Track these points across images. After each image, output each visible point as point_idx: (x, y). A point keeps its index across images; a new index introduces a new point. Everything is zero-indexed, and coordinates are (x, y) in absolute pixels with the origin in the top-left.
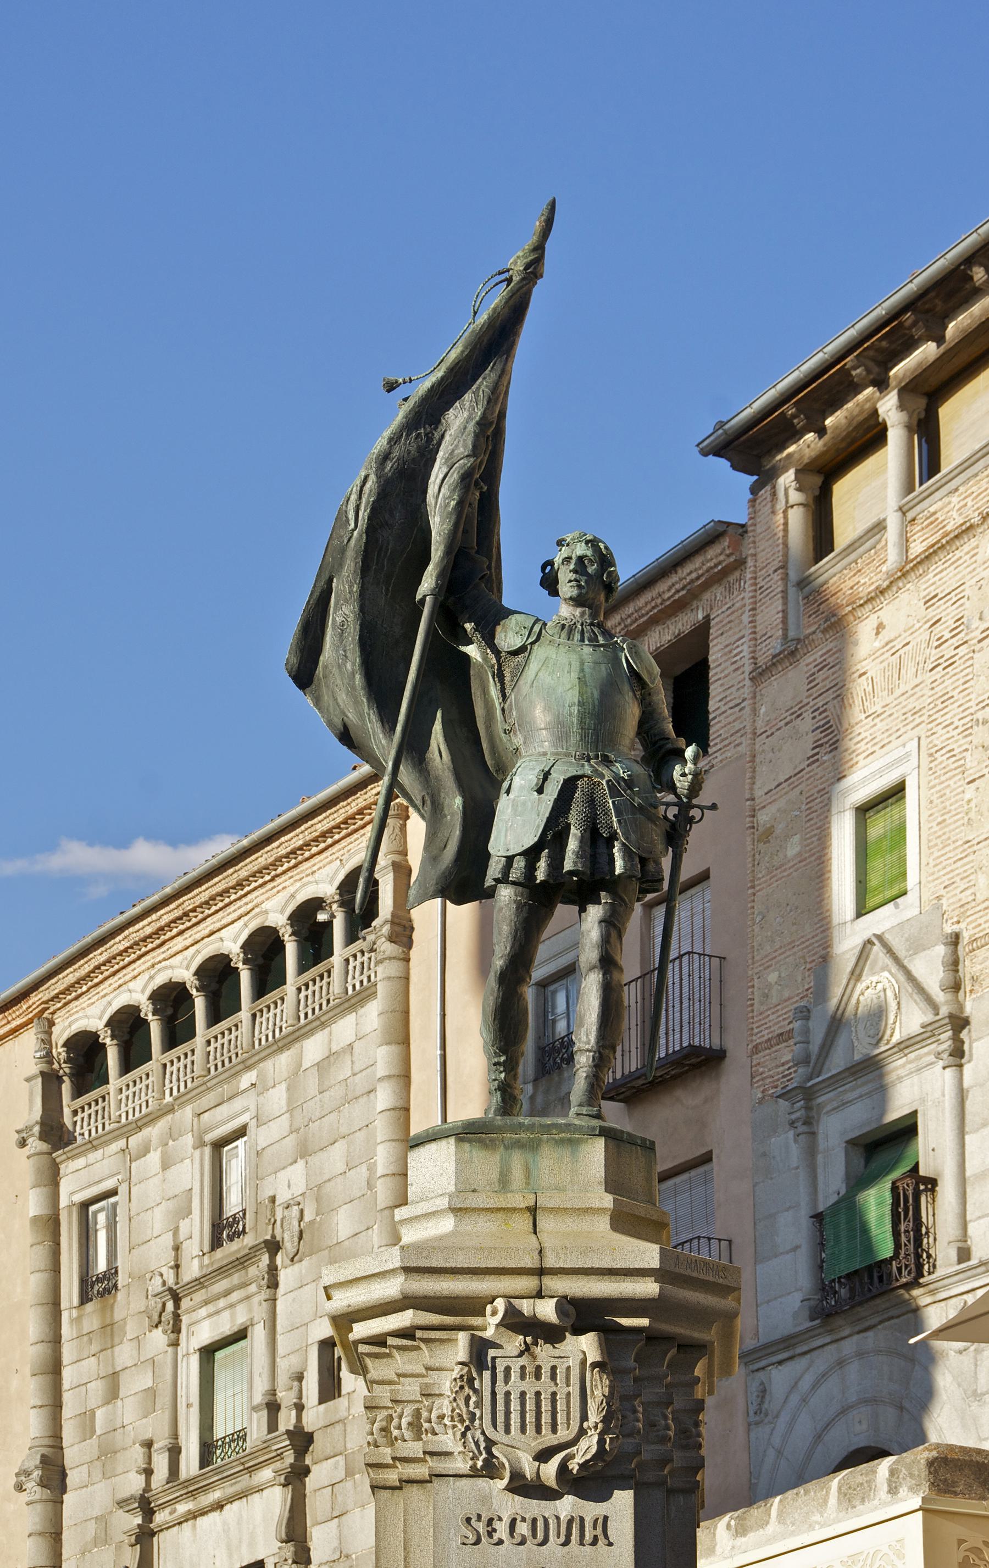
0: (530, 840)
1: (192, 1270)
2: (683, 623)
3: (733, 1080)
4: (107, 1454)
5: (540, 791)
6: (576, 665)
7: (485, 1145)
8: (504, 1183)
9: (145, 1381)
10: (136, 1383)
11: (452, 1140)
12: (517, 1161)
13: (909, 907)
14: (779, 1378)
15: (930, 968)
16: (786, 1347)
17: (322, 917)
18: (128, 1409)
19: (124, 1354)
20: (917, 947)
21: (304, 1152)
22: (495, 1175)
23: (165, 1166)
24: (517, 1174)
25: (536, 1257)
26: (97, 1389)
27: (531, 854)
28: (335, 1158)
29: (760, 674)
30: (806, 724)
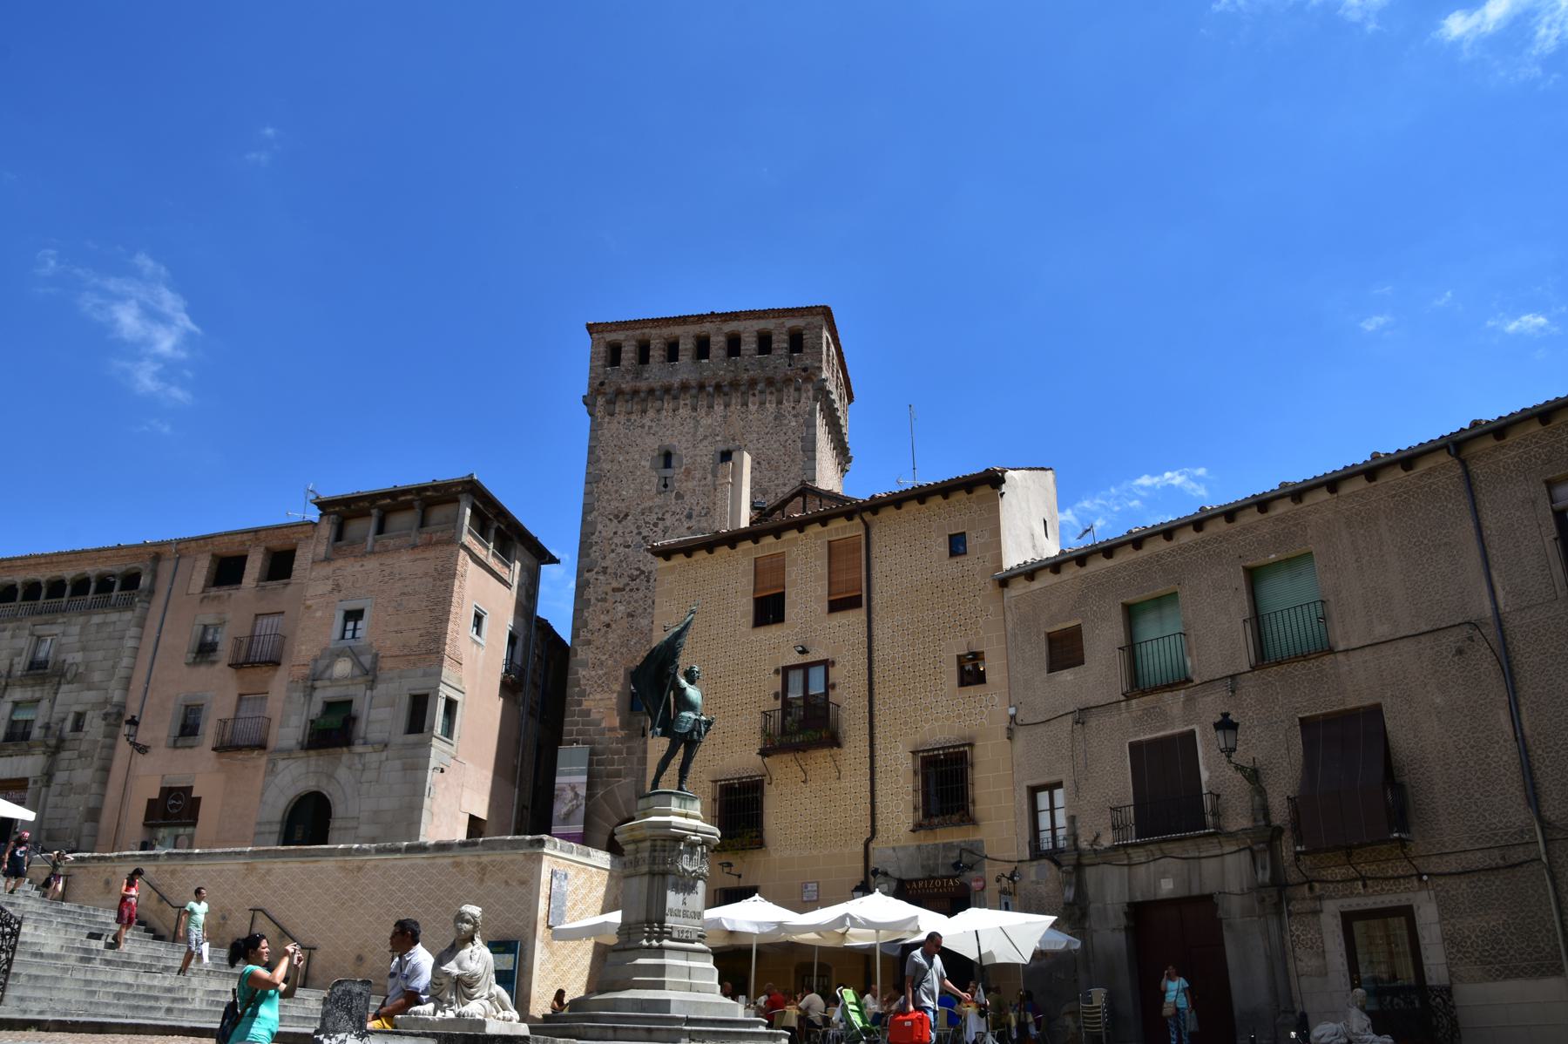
14: (281, 764)
15: (366, 660)
16: (287, 753)
23: (13, 637)
28: (100, 655)
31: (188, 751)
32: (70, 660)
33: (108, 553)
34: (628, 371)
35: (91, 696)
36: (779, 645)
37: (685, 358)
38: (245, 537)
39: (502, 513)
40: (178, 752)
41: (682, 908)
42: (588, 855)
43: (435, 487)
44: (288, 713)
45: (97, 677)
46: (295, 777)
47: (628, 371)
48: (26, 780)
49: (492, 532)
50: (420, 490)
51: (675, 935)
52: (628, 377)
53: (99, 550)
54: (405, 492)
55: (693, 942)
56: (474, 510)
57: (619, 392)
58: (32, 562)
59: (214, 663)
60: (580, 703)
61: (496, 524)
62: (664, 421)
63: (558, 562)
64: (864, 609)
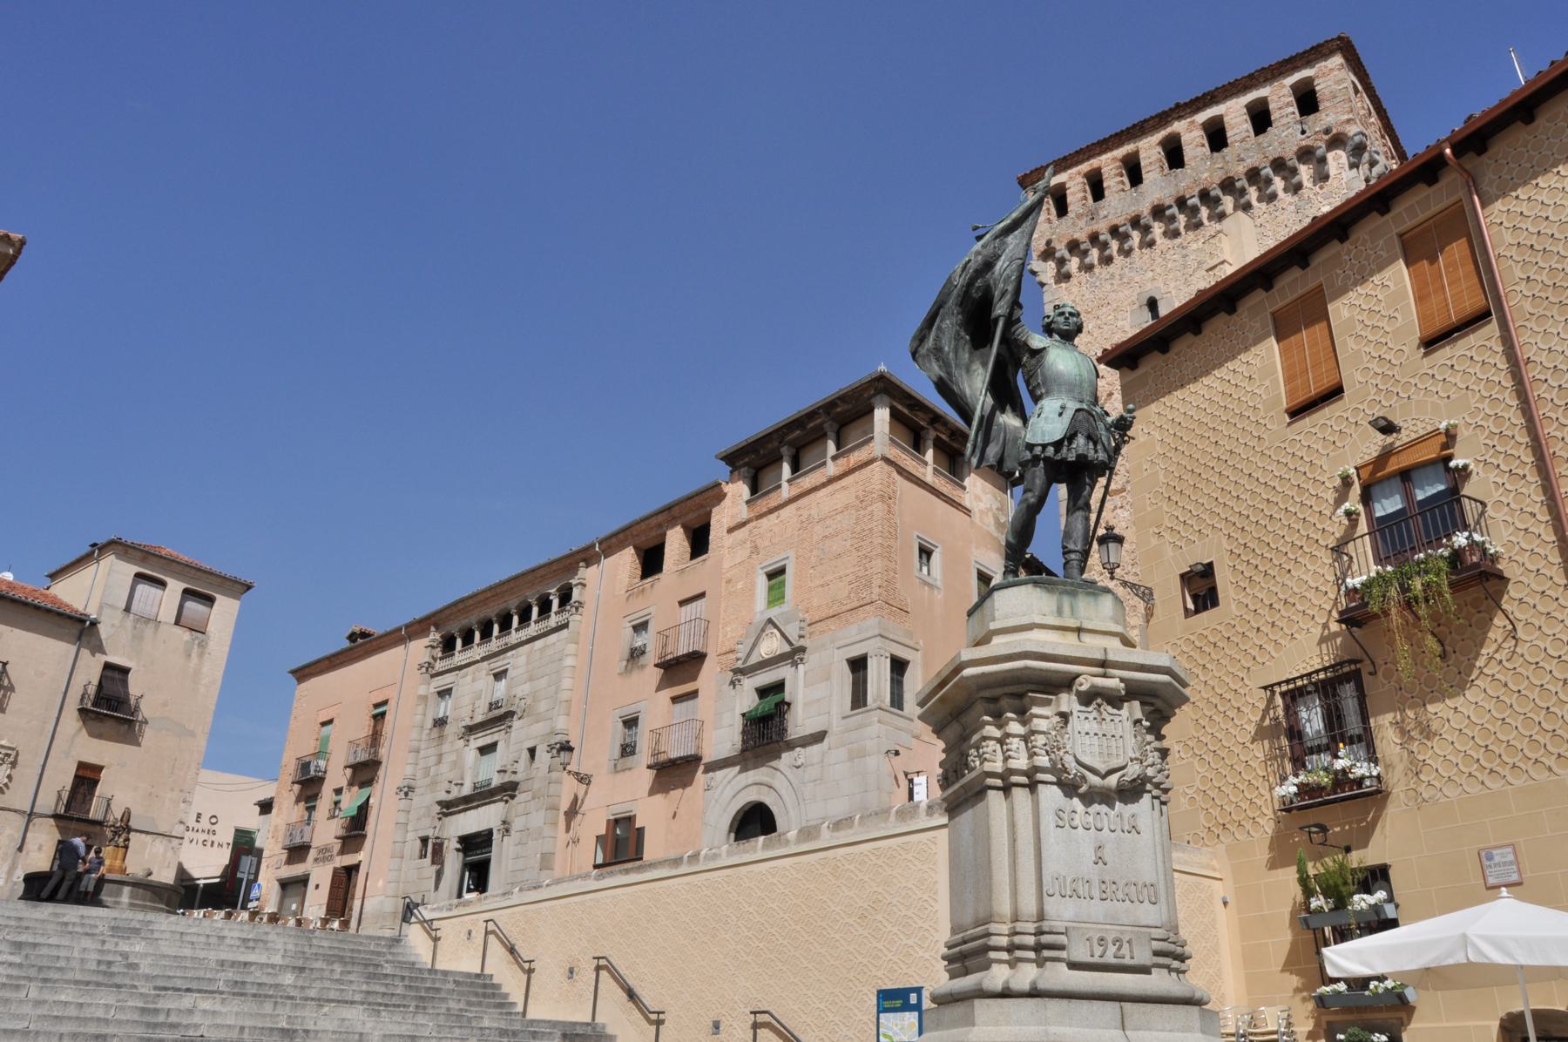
0: (1058, 437)
1: (479, 719)
2: (702, 511)
3: (708, 665)
4: (434, 783)
7: (1049, 591)
8: (1060, 612)
9: (453, 757)
10: (449, 759)
12: (1066, 601)
13: (785, 608)
18: (444, 768)
19: (446, 747)
20: (787, 622)
21: (531, 679)
22: (1055, 608)
24: (1066, 609)
26: (433, 759)
27: (1058, 445)
28: (543, 682)
29: (730, 531)
30: (749, 545)
32: (520, 694)
33: (542, 572)
34: (1079, 216)
35: (540, 728)
36: (1345, 442)
38: (660, 518)
40: (619, 776)
41: (1088, 868)
43: (843, 398)
44: (720, 714)
45: (543, 706)
46: (728, 792)
47: (1079, 216)
48: (490, 832)
49: (930, 443)
50: (829, 406)
51: (1080, 953)
52: (1082, 223)
53: (533, 571)
54: (812, 414)
55: (1144, 970)
56: (895, 415)
57: (1073, 246)
58: (481, 598)
59: (643, 666)
61: (932, 434)
64: (1494, 323)
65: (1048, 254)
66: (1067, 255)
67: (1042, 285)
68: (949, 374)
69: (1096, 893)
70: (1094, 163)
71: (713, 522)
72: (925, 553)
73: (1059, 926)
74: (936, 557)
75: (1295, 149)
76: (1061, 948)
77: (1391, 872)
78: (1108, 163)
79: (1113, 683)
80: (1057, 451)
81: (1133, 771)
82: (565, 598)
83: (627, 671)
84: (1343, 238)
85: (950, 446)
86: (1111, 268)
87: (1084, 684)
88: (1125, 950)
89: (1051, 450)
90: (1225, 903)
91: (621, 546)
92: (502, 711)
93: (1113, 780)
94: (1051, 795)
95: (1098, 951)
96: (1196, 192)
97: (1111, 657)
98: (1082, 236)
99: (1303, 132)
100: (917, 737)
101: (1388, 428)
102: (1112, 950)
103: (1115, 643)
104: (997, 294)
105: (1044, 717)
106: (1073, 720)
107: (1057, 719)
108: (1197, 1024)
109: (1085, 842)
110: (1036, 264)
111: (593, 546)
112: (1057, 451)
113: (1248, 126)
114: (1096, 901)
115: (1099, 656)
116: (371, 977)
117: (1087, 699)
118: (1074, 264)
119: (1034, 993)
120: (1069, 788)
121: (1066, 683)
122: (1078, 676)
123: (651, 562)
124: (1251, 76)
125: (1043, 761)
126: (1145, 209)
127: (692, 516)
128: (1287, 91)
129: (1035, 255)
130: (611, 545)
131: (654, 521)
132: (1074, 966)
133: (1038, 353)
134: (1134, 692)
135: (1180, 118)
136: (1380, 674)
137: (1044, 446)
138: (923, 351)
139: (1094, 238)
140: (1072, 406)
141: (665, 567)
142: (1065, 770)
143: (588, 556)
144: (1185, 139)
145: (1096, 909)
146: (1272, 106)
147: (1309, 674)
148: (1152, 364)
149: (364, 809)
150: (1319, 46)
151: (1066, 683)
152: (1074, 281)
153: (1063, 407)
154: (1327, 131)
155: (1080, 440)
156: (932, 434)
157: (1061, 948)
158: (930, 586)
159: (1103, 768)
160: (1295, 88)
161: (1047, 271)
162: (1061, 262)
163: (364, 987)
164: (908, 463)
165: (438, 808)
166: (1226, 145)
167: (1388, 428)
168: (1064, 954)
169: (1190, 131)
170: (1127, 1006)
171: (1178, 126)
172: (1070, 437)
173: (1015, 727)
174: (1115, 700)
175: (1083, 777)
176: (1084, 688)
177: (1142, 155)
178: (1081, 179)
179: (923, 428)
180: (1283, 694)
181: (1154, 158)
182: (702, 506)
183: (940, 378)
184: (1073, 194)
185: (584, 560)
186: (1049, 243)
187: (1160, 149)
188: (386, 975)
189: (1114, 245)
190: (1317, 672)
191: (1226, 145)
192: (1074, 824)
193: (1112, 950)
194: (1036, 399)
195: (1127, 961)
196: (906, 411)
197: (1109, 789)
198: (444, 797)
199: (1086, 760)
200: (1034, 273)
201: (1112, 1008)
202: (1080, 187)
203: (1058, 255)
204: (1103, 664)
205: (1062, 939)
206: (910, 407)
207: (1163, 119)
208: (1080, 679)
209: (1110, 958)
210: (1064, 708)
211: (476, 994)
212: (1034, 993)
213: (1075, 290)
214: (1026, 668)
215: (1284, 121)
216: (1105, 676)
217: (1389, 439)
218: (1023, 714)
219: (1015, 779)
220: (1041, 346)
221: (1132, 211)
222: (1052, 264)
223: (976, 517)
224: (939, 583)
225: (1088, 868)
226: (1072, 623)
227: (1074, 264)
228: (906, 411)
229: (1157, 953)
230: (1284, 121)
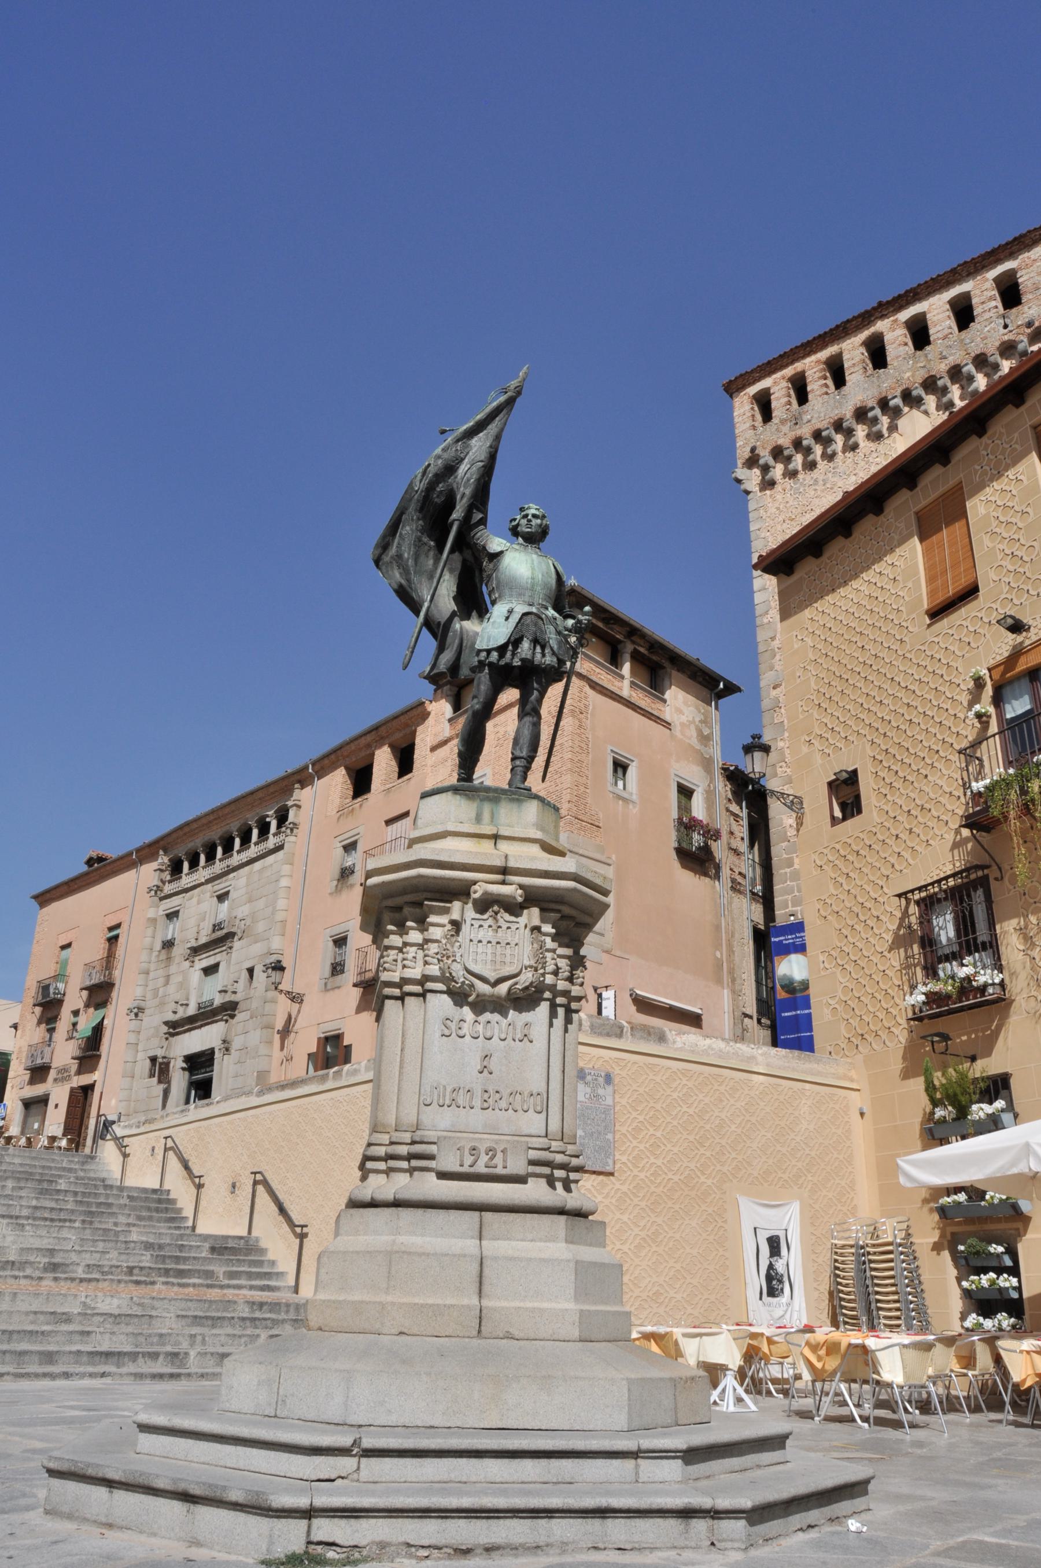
0: (502, 641)
1: (203, 940)
4: (162, 1004)
5: (507, 618)
6: (529, 561)
7: (469, 798)
8: (478, 819)
9: (180, 978)
10: (175, 980)
11: (450, 793)
12: (487, 808)
17: (268, 820)
18: (172, 988)
19: (173, 969)
21: (250, 901)
22: (473, 815)
23: (199, 903)
25: (503, 860)
26: (161, 981)
27: (502, 649)
28: (261, 904)
31: (336, 991)
32: (240, 916)
33: (260, 794)
34: (783, 422)
35: (258, 949)
37: (854, 377)
39: (633, 632)
41: (470, 1077)
42: (662, 1038)
45: (261, 927)
47: (783, 422)
48: (212, 1052)
49: (627, 656)
51: (449, 1162)
52: (785, 429)
53: (252, 793)
55: (521, 1180)
57: (777, 453)
58: (204, 821)
59: (352, 886)
60: (790, 863)
61: (629, 647)
62: (841, 469)
63: (739, 690)
65: (752, 461)
66: (771, 461)
67: (747, 493)
68: (408, 580)
69: (477, 1103)
70: (798, 366)
71: (417, 741)
72: (620, 767)
73: (431, 1135)
74: (632, 772)
75: (997, 344)
76: (431, 1157)
77: (1012, 1081)
78: (812, 365)
79: (510, 890)
80: (502, 656)
81: (527, 978)
82: (282, 818)
83: (338, 890)
84: (981, 432)
85: (649, 659)
86: (816, 474)
87: (477, 892)
88: (498, 1160)
89: (495, 655)
90: (862, 1114)
91: (333, 767)
92: (224, 931)
93: (503, 988)
94: (441, 1004)
95: (468, 1160)
96: (898, 393)
97: (512, 864)
98: (785, 441)
99: (1006, 326)
100: (607, 952)
101: (1017, 627)
102: (484, 1159)
103: (535, 850)
104: (458, 497)
105: (439, 925)
106: (465, 928)
107: (449, 927)
108: (562, 1233)
109: (471, 1052)
110: (741, 473)
111: (307, 767)
112: (502, 656)
113: (952, 323)
114: (477, 1110)
115: (499, 862)
116: (43, 1192)
117: (484, 905)
118: (778, 471)
119: (397, 1204)
120: (459, 996)
121: (460, 892)
122: (475, 883)
123: (361, 782)
124: (953, 271)
125: (434, 970)
126: (847, 411)
127: (398, 735)
128: (990, 284)
129: (740, 463)
130: (323, 766)
131: (363, 741)
132: (443, 1175)
133: (496, 556)
134: (533, 898)
135: (883, 317)
136: (1006, 879)
137: (489, 652)
138: (386, 558)
139: (797, 443)
140: (520, 609)
141: (373, 787)
142: (452, 979)
143: (302, 778)
144: (888, 338)
145: (476, 1119)
146: (974, 301)
147: (939, 881)
148: (807, 568)
149: (98, 1031)
150: (1021, 236)
151: (460, 892)
152: (778, 488)
153: (510, 612)
154: (1029, 324)
155: (526, 645)
156: (629, 647)
157: (431, 1157)
158: (625, 800)
159: (492, 976)
160: (998, 281)
161: (752, 478)
162: (766, 469)
163: (34, 1203)
164: (603, 677)
165: (165, 1029)
166: (928, 343)
167: (1017, 627)
168: (432, 1164)
169: (893, 331)
170: (488, 1216)
171: (880, 325)
172: (515, 642)
173: (415, 936)
174: (514, 908)
175: (472, 986)
176: (476, 896)
177: (845, 357)
178: (785, 384)
179: (620, 642)
180: (918, 903)
181: (857, 359)
182: (407, 725)
183: (401, 586)
184: (778, 399)
185: (299, 782)
186: (753, 450)
187: (863, 350)
188: (58, 1191)
189: (818, 450)
190: (946, 878)
191: (928, 343)
192: (461, 1033)
193: (484, 1159)
194: (493, 603)
195: (500, 1171)
196: (600, 624)
197: (499, 997)
198: (171, 1017)
199: (476, 969)
200: (739, 481)
201: (471, 1218)
202: (784, 392)
203: (762, 462)
204: (504, 871)
205: (433, 1149)
206: (603, 620)
207: (866, 318)
208: (474, 888)
209: (481, 1168)
210: (455, 915)
211: (149, 1209)
212: (397, 1204)
213: (779, 497)
214: (420, 876)
215: (987, 315)
216: (503, 883)
217: (1019, 638)
218: (422, 924)
219: (408, 988)
220: (499, 549)
221: (835, 414)
222: (757, 472)
223: (677, 731)
224: (634, 797)
225: (470, 1077)
226: (489, 830)
227: (778, 471)
228: (600, 624)
229: (532, 1163)
230: (987, 315)
